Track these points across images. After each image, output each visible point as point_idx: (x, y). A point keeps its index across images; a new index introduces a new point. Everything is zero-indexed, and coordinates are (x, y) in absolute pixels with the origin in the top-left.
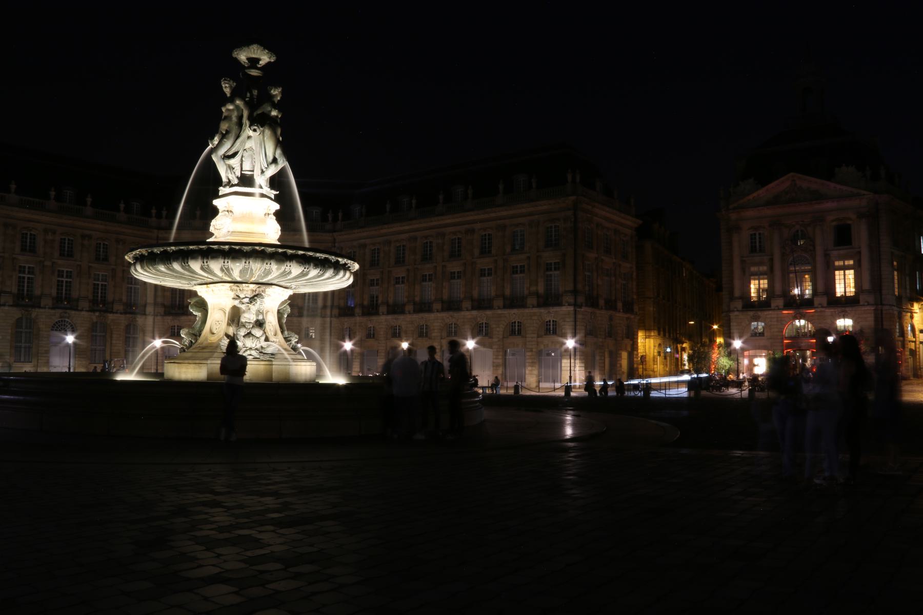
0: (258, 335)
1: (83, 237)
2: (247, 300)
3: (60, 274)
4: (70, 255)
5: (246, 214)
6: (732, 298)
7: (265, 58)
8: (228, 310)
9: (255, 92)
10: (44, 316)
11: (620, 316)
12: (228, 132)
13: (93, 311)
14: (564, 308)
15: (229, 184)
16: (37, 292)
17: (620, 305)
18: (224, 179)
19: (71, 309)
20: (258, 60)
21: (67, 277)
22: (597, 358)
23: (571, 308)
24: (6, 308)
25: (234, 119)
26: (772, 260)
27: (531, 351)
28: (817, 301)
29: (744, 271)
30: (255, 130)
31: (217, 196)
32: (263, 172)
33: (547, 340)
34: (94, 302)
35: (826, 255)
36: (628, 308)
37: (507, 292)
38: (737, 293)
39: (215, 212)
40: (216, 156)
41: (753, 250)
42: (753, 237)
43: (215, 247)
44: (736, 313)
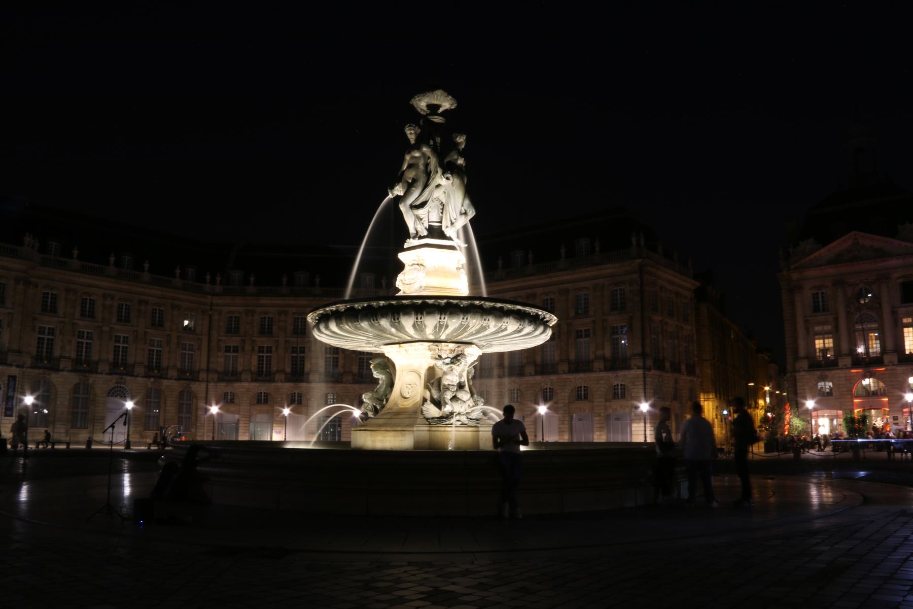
0: (465, 399)
1: (140, 302)
2: (448, 361)
3: (117, 340)
4: (127, 320)
5: (436, 266)
6: (796, 358)
7: (446, 104)
8: (423, 372)
9: (438, 140)
10: (101, 382)
11: (684, 378)
12: (415, 181)
13: (148, 377)
14: (633, 372)
15: (418, 236)
16: (95, 357)
17: (683, 367)
18: (412, 231)
19: (127, 374)
20: (439, 106)
21: (124, 342)
23: (640, 372)
24: (65, 373)
25: (421, 167)
26: (836, 319)
27: (600, 416)
28: (887, 359)
29: (807, 330)
30: (448, 179)
31: (404, 250)
32: (452, 223)
33: (616, 404)
34: (149, 368)
35: (894, 313)
36: (691, 371)
37: (572, 356)
38: (802, 353)
39: (400, 267)
40: (405, 206)
41: (816, 309)
42: (815, 296)
43: (430, 301)
44: (803, 373)
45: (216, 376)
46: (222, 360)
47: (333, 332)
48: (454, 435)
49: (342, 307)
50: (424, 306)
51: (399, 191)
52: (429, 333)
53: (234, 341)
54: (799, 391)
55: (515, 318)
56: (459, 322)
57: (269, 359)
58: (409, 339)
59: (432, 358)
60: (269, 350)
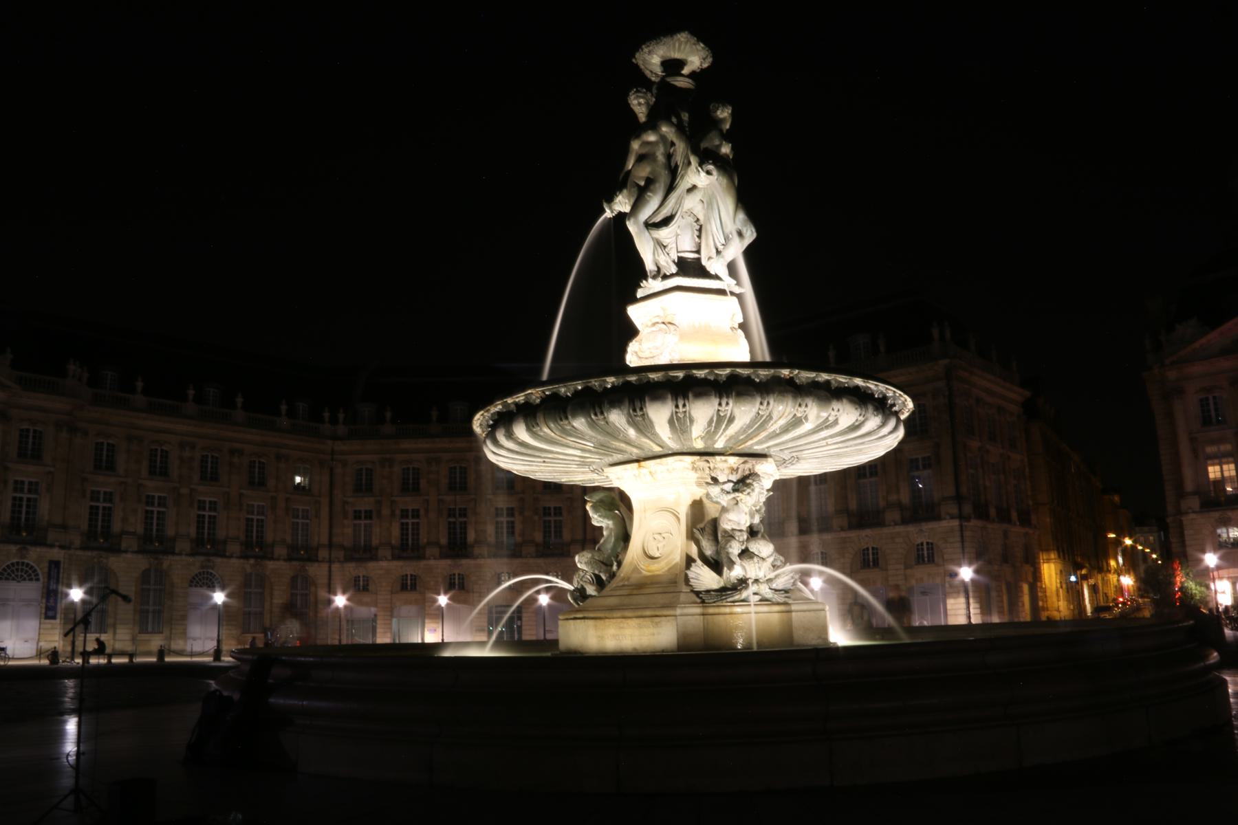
0: (764, 555)
1: (232, 452)
2: (729, 487)
3: (201, 505)
4: (215, 478)
6: (1181, 494)
7: (695, 58)
8: (683, 510)
9: (685, 117)
10: (180, 566)
11: (1016, 530)
12: (650, 182)
13: (245, 557)
14: (944, 524)
15: (660, 274)
17: (1014, 515)
18: (650, 266)
19: (216, 555)
20: (681, 64)
21: (210, 509)
22: (994, 594)
23: (956, 523)
24: (129, 556)
25: (661, 158)
29: (1195, 452)
30: (708, 173)
31: (634, 300)
32: (718, 252)
33: (920, 572)
36: (1025, 520)
38: (1189, 486)
40: (636, 223)
41: (1206, 421)
42: (1204, 403)
44: (1192, 516)
45: (341, 554)
46: (349, 531)
47: (523, 444)
48: (748, 621)
49: (535, 394)
50: (686, 383)
51: (622, 204)
52: (697, 437)
53: (365, 503)
54: (1187, 543)
55: (852, 401)
56: (755, 410)
57: (416, 527)
58: (657, 449)
59: (699, 484)
60: (416, 514)
